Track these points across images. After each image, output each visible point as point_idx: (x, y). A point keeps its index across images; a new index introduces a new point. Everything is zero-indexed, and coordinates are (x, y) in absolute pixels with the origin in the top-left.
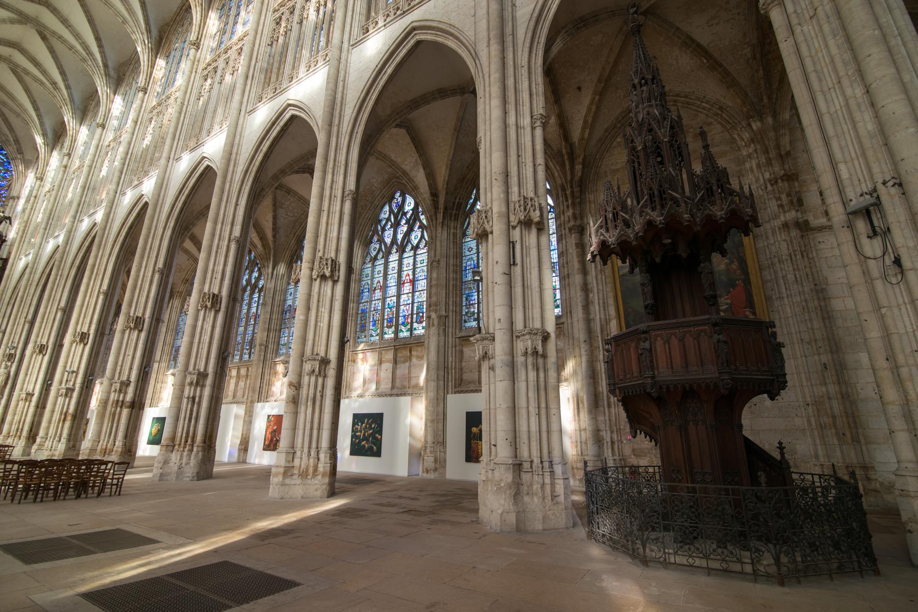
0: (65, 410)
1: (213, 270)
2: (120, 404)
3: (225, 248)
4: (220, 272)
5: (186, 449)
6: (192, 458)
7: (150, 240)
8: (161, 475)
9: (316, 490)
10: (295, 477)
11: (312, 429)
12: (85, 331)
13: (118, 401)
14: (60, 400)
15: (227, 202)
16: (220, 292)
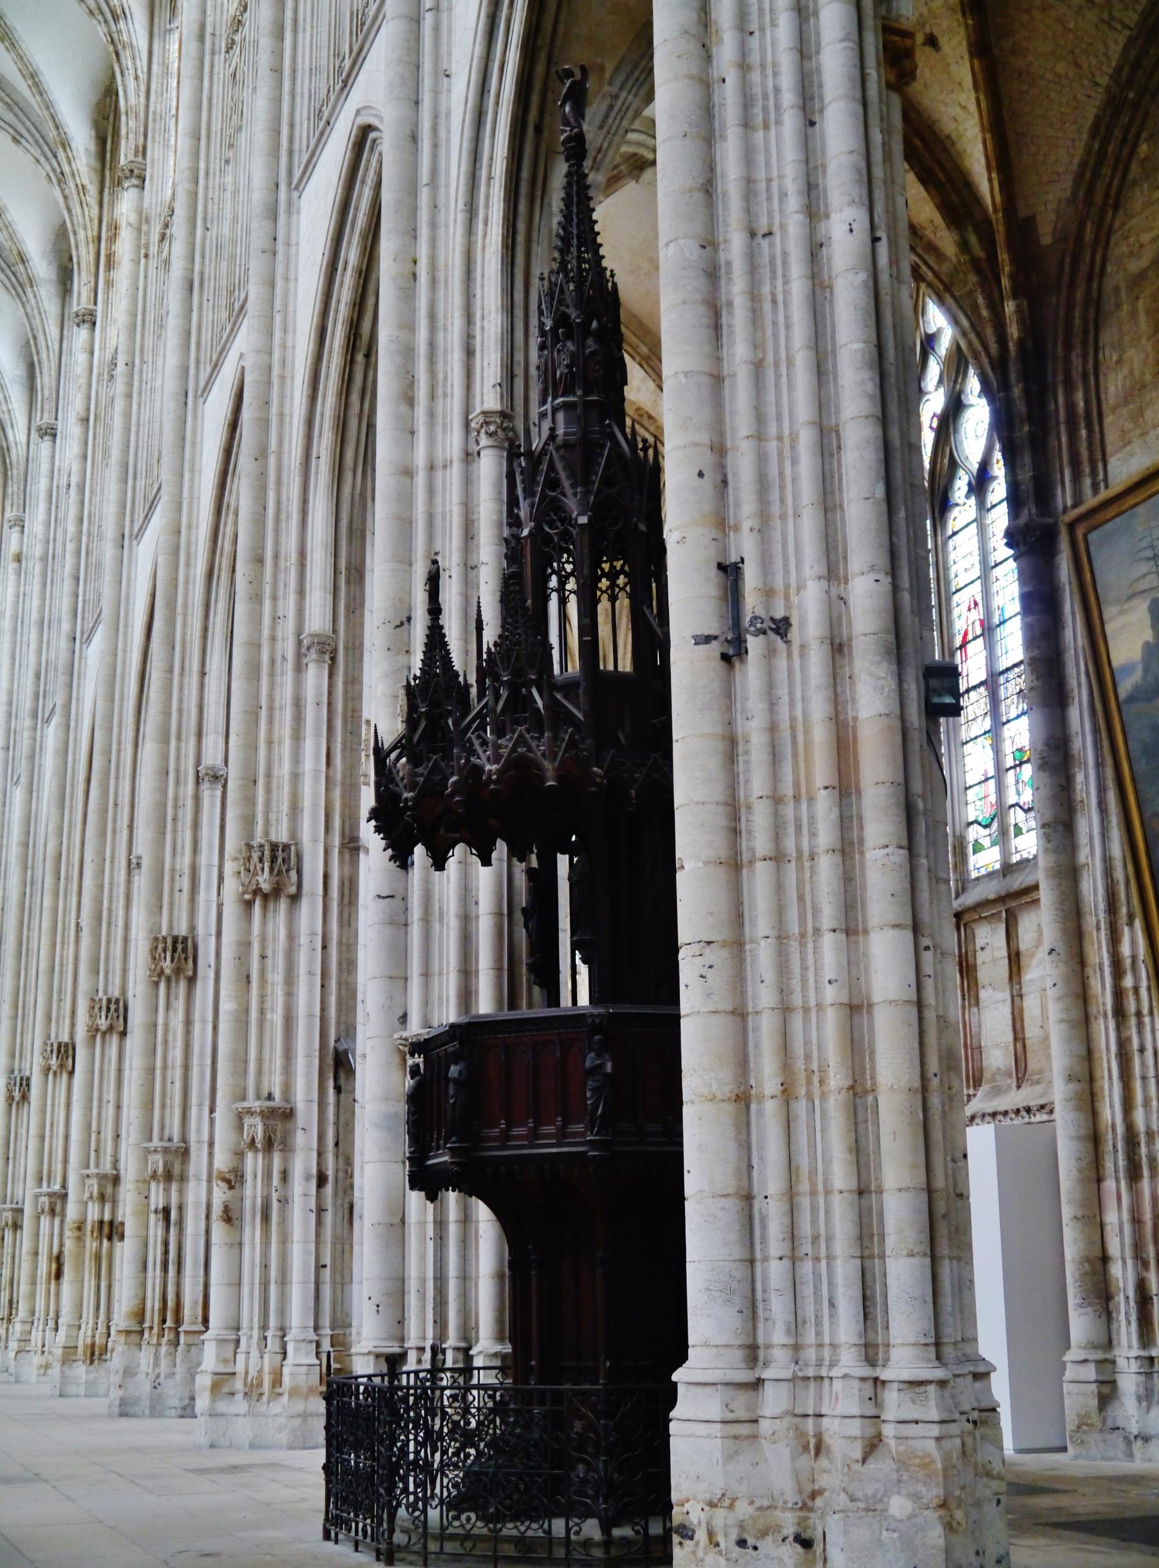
0: (55, 1250)
1: (173, 870)
2: (106, 1230)
3: (189, 803)
4: (187, 871)
5: (164, 1340)
6: (178, 1361)
7: (112, 781)
8: (123, 1402)
9: (279, 1430)
10: (239, 1397)
11: (265, 1284)
12: (65, 1038)
13: (101, 1223)
14: (45, 1221)
15: (182, 674)
16: (192, 928)
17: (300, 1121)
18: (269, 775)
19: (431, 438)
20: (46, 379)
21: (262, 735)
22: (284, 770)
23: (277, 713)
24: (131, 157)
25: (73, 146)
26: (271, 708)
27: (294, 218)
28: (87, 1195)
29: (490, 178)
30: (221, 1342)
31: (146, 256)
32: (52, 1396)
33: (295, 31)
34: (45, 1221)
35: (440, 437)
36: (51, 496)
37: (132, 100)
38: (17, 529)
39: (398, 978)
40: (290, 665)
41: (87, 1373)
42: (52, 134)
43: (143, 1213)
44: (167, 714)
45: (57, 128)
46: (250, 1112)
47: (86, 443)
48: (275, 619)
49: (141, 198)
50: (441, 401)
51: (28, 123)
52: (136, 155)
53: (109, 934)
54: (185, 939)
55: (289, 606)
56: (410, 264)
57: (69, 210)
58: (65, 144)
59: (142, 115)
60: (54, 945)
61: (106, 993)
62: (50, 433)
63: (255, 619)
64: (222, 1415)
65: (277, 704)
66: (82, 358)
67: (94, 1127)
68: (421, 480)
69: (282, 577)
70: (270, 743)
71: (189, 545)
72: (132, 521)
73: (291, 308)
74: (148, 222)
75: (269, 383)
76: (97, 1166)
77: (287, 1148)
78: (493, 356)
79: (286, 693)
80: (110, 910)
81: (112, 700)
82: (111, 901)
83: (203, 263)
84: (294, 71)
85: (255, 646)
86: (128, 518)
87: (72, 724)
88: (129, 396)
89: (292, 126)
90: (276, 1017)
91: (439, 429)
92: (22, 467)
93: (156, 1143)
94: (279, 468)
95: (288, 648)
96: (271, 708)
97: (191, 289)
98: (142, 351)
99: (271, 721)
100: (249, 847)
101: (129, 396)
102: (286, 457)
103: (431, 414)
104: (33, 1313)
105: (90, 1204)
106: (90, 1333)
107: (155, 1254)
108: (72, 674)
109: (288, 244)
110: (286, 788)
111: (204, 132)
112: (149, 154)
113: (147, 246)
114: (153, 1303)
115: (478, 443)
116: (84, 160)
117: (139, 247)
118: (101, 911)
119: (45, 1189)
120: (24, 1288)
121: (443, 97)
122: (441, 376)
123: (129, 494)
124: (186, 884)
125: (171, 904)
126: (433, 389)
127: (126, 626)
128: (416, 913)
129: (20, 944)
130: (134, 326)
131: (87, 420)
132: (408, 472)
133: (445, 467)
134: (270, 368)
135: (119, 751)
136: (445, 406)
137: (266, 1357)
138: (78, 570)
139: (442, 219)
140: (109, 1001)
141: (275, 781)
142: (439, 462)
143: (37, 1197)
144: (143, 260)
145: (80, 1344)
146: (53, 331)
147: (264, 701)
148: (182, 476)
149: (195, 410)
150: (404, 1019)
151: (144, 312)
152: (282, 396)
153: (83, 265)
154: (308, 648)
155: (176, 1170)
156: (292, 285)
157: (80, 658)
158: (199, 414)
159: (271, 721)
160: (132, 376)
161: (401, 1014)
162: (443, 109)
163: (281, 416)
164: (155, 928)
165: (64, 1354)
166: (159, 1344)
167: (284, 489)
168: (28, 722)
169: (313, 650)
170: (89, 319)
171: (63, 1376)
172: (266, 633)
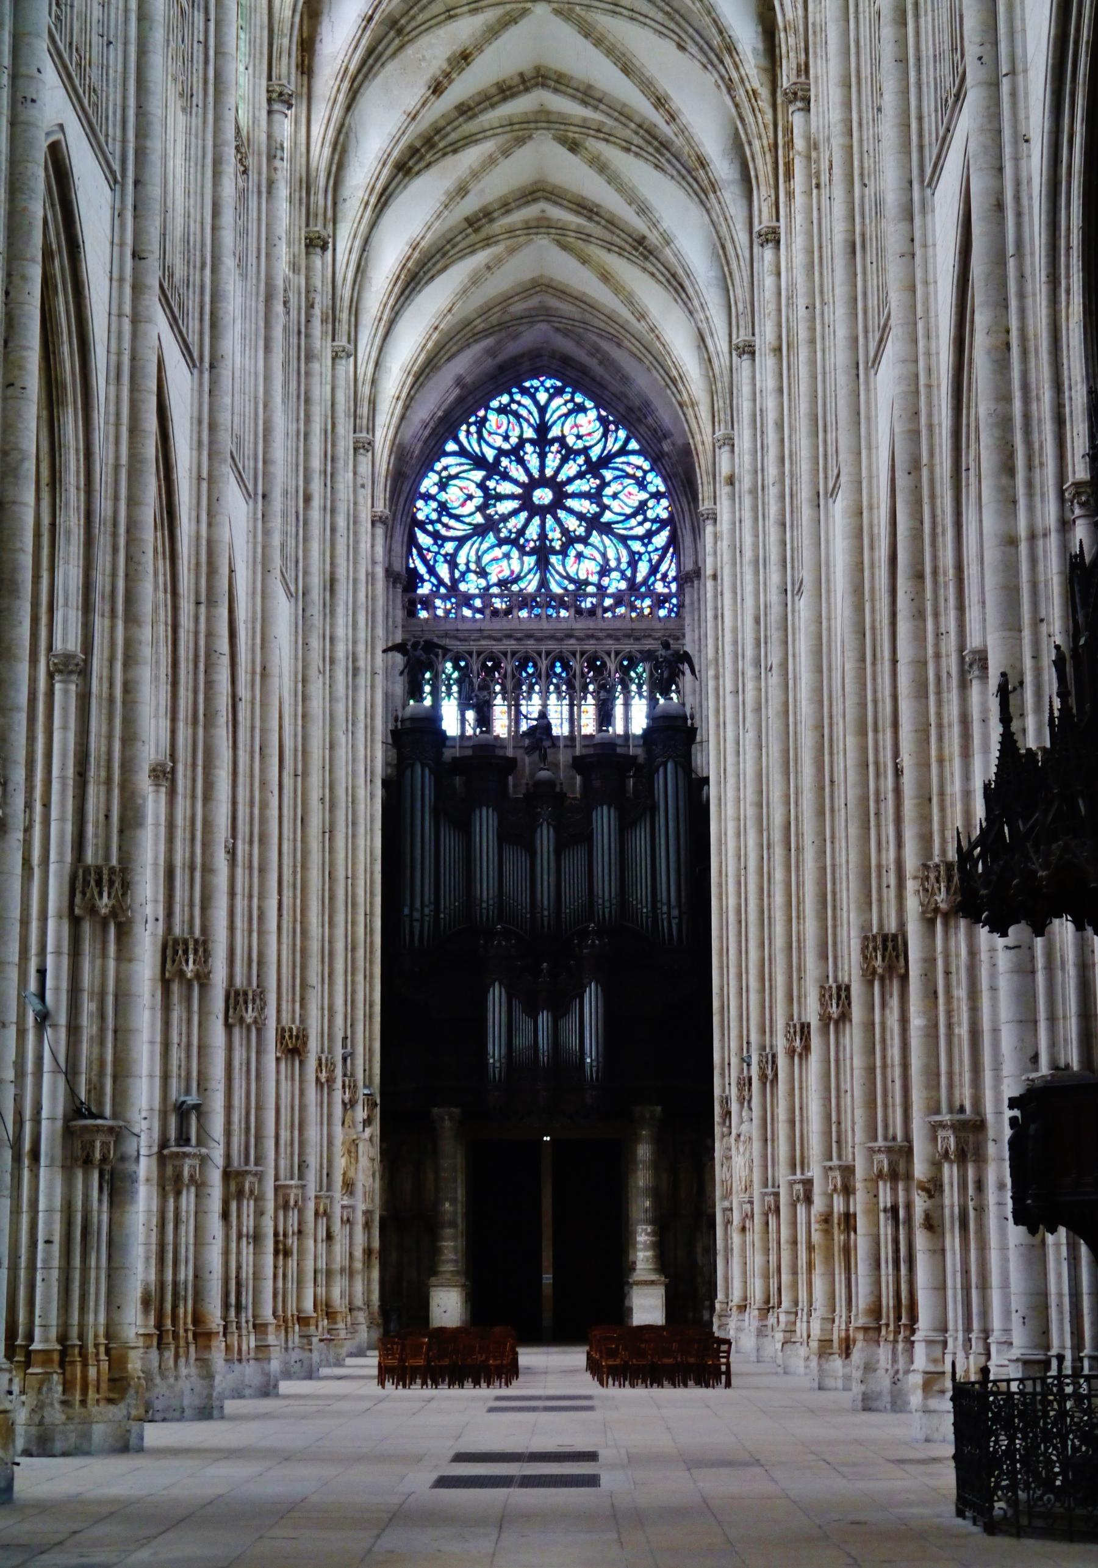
1: (879, 866)
3: (890, 796)
4: (892, 867)
5: (901, 1337)
7: (827, 758)
8: (866, 1397)
14: (801, 1209)
15: (874, 664)
16: (902, 925)
17: (991, 1133)
18: (942, 794)
19: (1031, 509)
20: (739, 291)
21: (933, 753)
22: (955, 788)
23: (946, 730)
24: (793, 79)
25: (740, 49)
26: (940, 726)
27: (929, 217)
28: (831, 1187)
29: (1069, 248)
30: (930, 1343)
31: (818, 186)
32: (812, 1389)
33: (917, 16)
34: (801, 1209)
35: (1039, 505)
36: (755, 421)
37: (790, 15)
38: (727, 448)
39: (1027, 1022)
40: (954, 682)
41: (844, 1366)
42: (716, 41)
43: (873, 1211)
44: (863, 705)
45: (721, 32)
46: (942, 1125)
47: (781, 374)
48: (938, 635)
49: (808, 122)
50: (1038, 470)
51: (691, 30)
52: (798, 76)
53: (834, 918)
54: (895, 936)
55: (950, 622)
56: (1003, 336)
57: (742, 120)
58: (731, 48)
59: (801, 29)
60: (790, 920)
61: (836, 980)
62: (748, 350)
63: (919, 637)
64: (934, 1411)
65: (945, 721)
66: (769, 281)
67: (834, 1118)
68: (1023, 548)
69: (942, 592)
70: (941, 761)
71: (871, 527)
72: (826, 478)
73: (932, 314)
74: (816, 148)
75: (917, 392)
76: (840, 1157)
77: (980, 1159)
78: (1081, 426)
79: (953, 711)
80: (834, 893)
81: (821, 671)
82: (834, 884)
83: (863, 223)
84: (918, 59)
85: (920, 663)
86: (821, 475)
87: (791, 683)
88: (812, 341)
89: (920, 119)
90: (963, 1031)
91: (1038, 498)
92: (726, 379)
93: (880, 1142)
94: (932, 481)
95: (951, 663)
96: (940, 726)
97: (854, 252)
98: (822, 292)
99: (940, 739)
100: (925, 867)
101: (812, 341)
102: (937, 469)
103: (1030, 484)
104: (796, 1303)
105: (835, 1196)
106: (843, 1327)
107: (886, 1252)
108: (786, 630)
109: (925, 246)
110: (959, 807)
111: (854, 80)
112: (812, 71)
113: (818, 177)
114: (888, 1301)
115: (1073, 512)
116: (753, 62)
117: (809, 176)
118: (825, 895)
119: (799, 1176)
120: (785, 1278)
121: (1023, 163)
122: (1036, 446)
123: (821, 449)
124: (892, 881)
125: (880, 901)
126: (1029, 458)
127: (828, 591)
128: (1040, 962)
129: (762, 912)
130: (811, 264)
131: (780, 349)
132: (1012, 541)
133: (1045, 535)
134: (917, 376)
135: (831, 725)
136: (1041, 475)
137: (971, 1357)
138: (784, 515)
139: (1029, 288)
140: (839, 988)
141: (948, 798)
142: (1040, 531)
143: (791, 1184)
144: (815, 191)
145: (835, 1337)
146: (742, 237)
147: (933, 719)
148: (859, 453)
149: (867, 383)
150: (1035, 1059)
151: (820, 247)
152: (930, 405)
153: (762, 179)
154: (971, 665)
155: (902, 1168)
156: (931, 288)
157: (793, 611)
158: (872, 387)
159: (940, 739)
160: (813, 319)
161: (1032, 1054)
162: (1024, 175)
163: (930, 427)
164: (866, 927)
165: (820, 1348)
166: (895, 1341)
167: (939, 501)
168: (750, 672)
169: (975, 667)
170: (772, 238)
171: (821, 1370)
172: (930, 651)
